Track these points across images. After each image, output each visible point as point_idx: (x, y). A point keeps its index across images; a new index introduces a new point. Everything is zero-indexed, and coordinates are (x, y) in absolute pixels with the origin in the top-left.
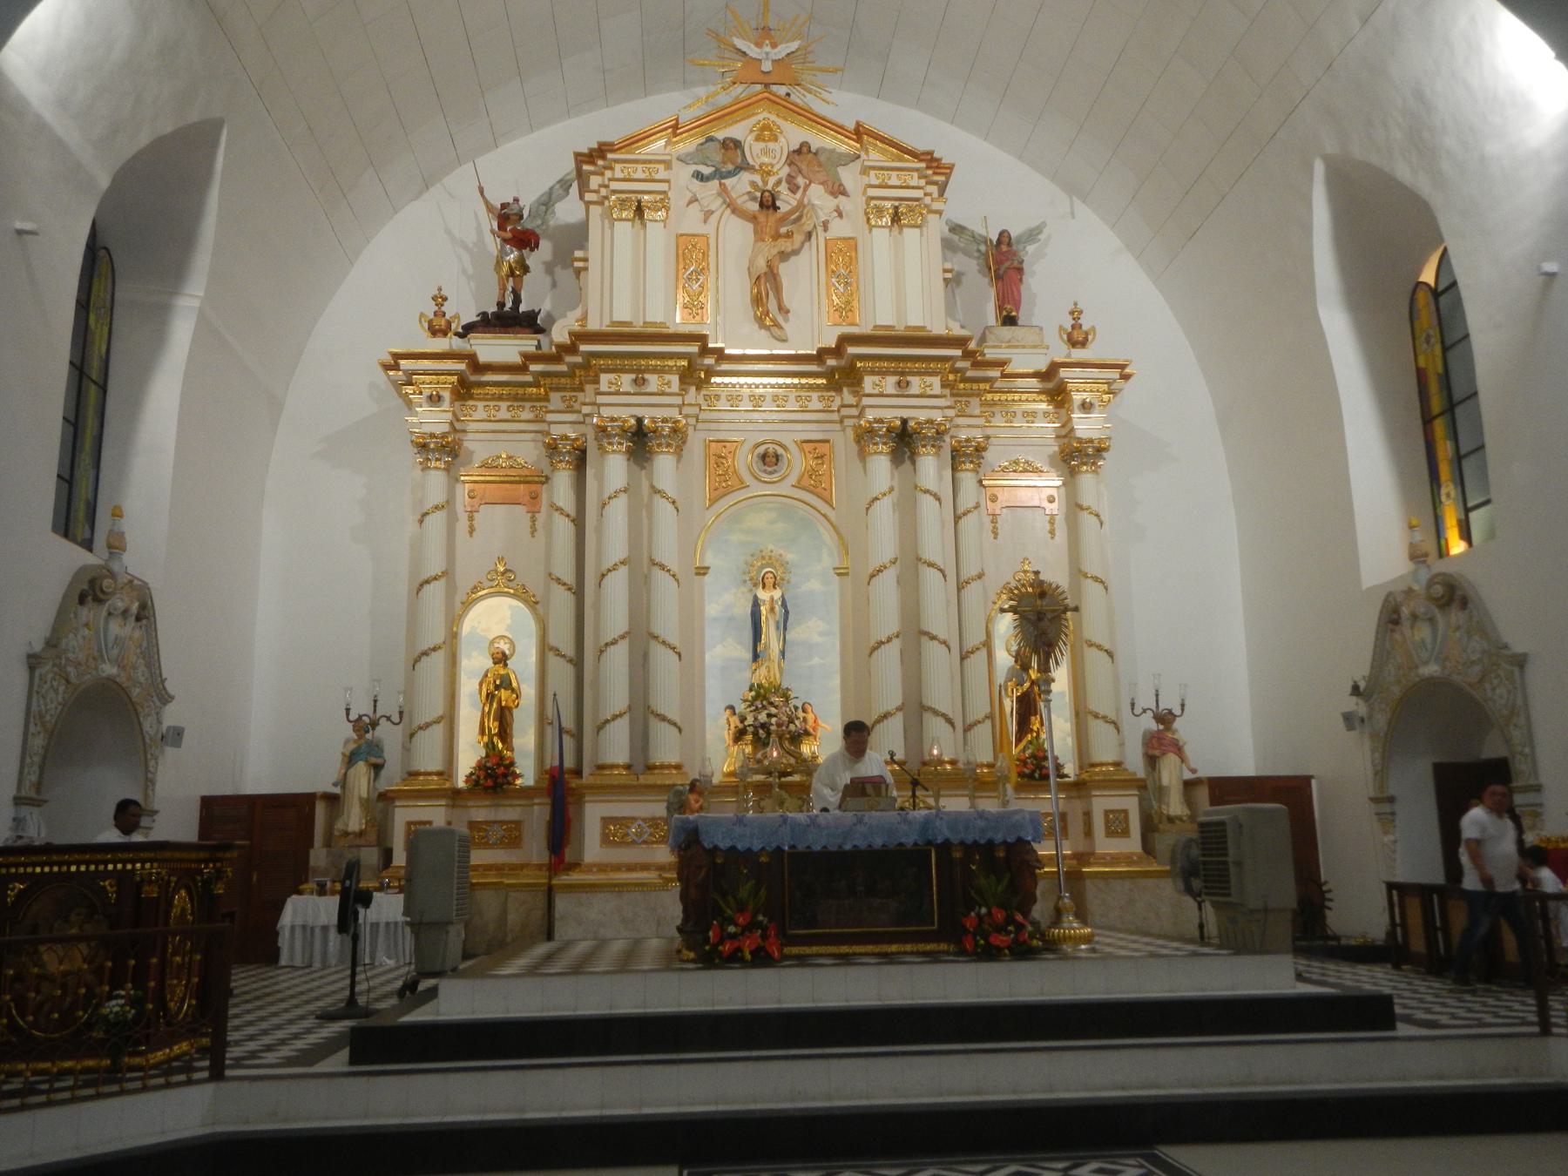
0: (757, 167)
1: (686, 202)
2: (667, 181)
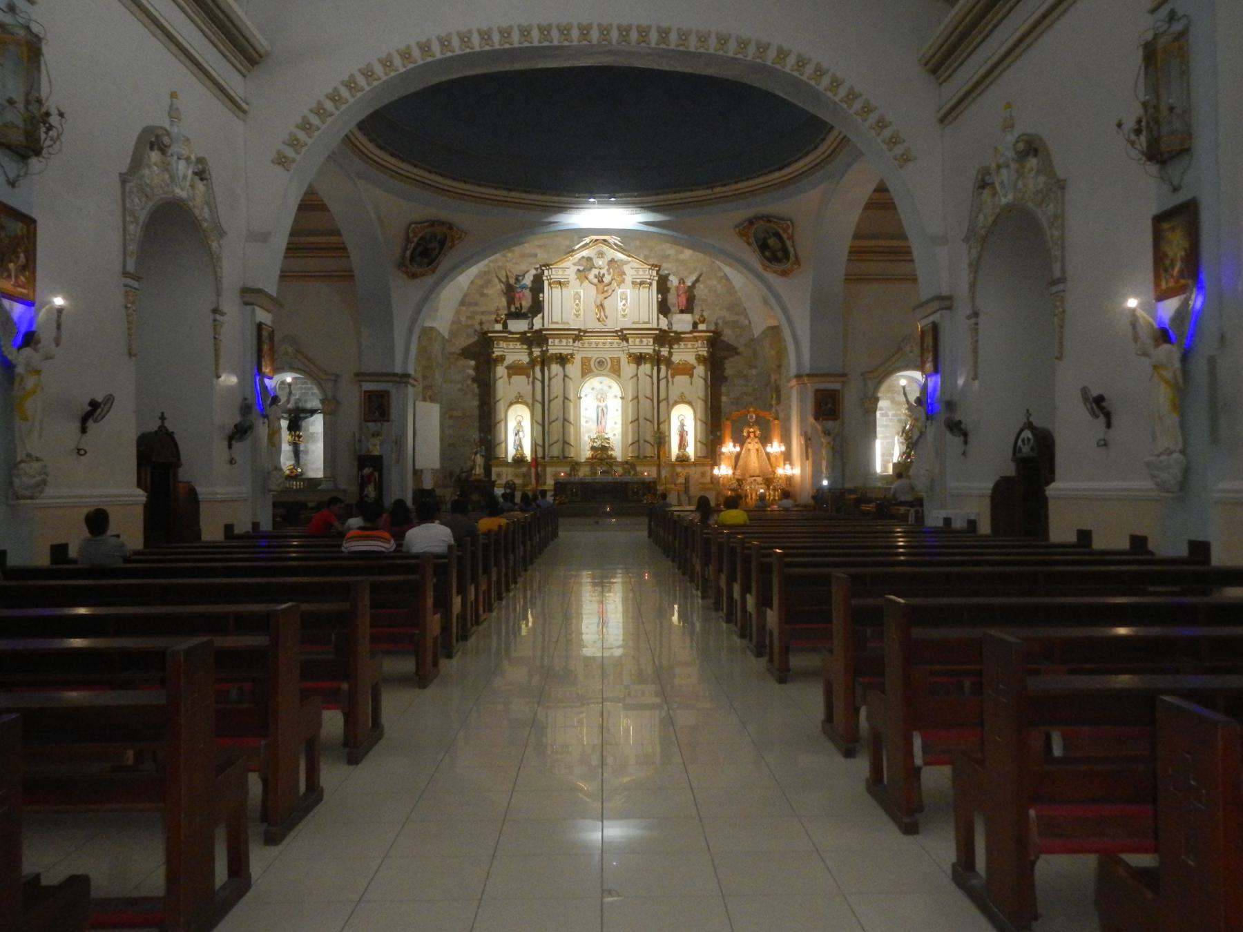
2: (569, 275)
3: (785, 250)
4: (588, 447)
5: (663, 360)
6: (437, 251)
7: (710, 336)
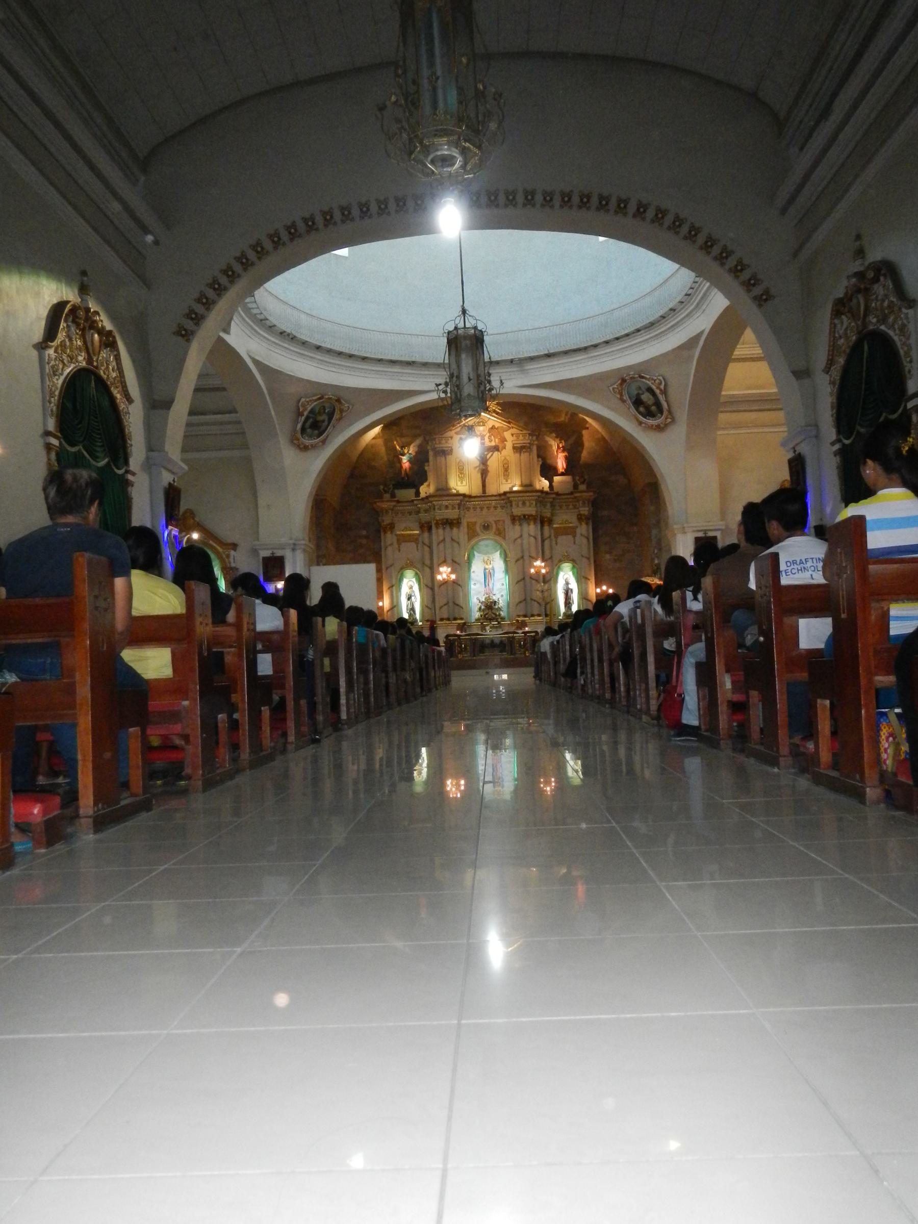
3: (658, 404)
4: (477, 608)
6: (326, 423)
7: (591, 496)
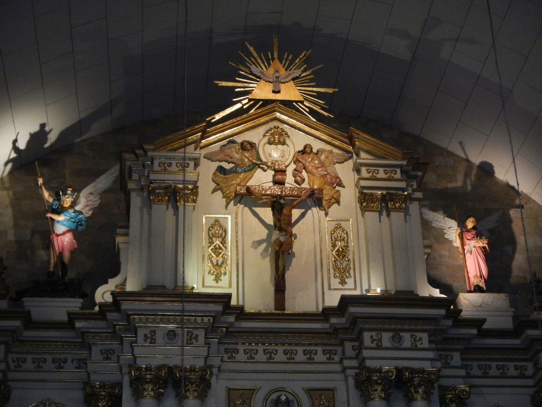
0: (269, 164)
1: (211, 189)
5: (451, 400)
